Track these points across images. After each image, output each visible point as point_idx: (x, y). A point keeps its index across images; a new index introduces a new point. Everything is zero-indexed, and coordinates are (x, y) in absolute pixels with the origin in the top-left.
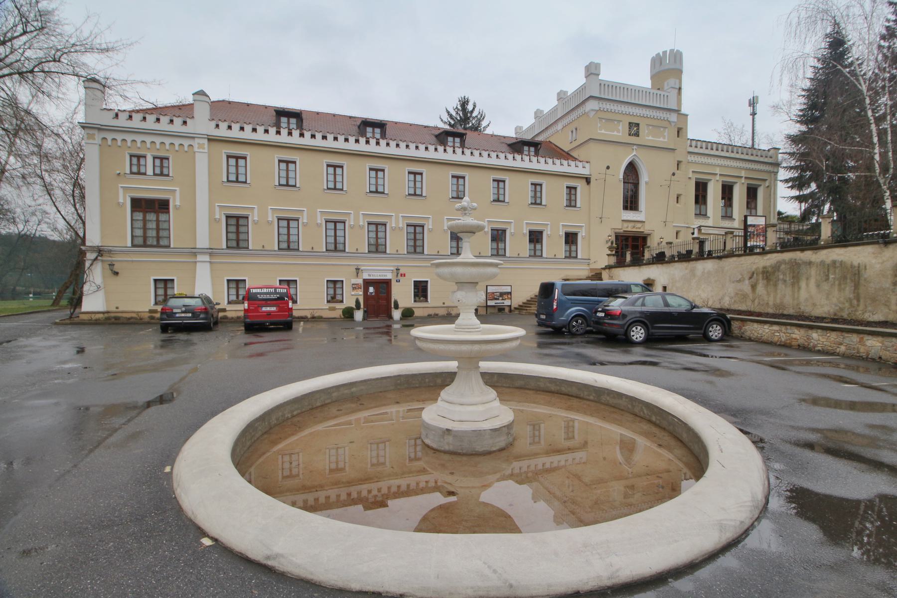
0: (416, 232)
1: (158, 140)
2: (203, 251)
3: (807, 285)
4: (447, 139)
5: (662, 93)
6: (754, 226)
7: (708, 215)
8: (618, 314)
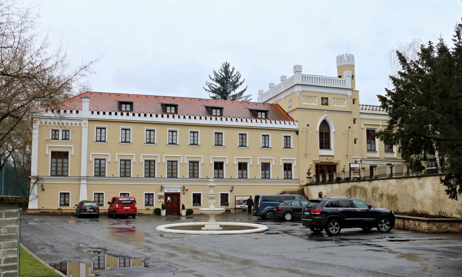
0: (194, 165)
2: (84, 178)
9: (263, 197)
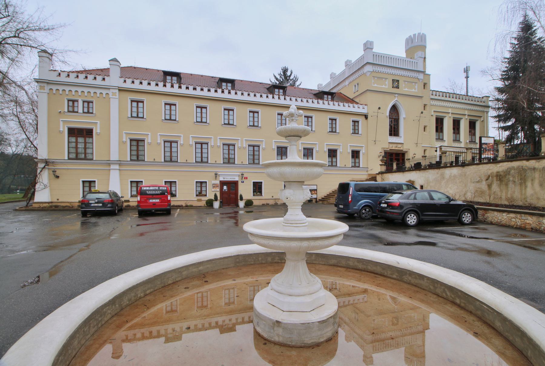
0: (254, 148)
1: (86, 90)
3: (532, 184)
4: (275, 90)
5: (414, 61)
6: (486, 144)
8: (397, 205)
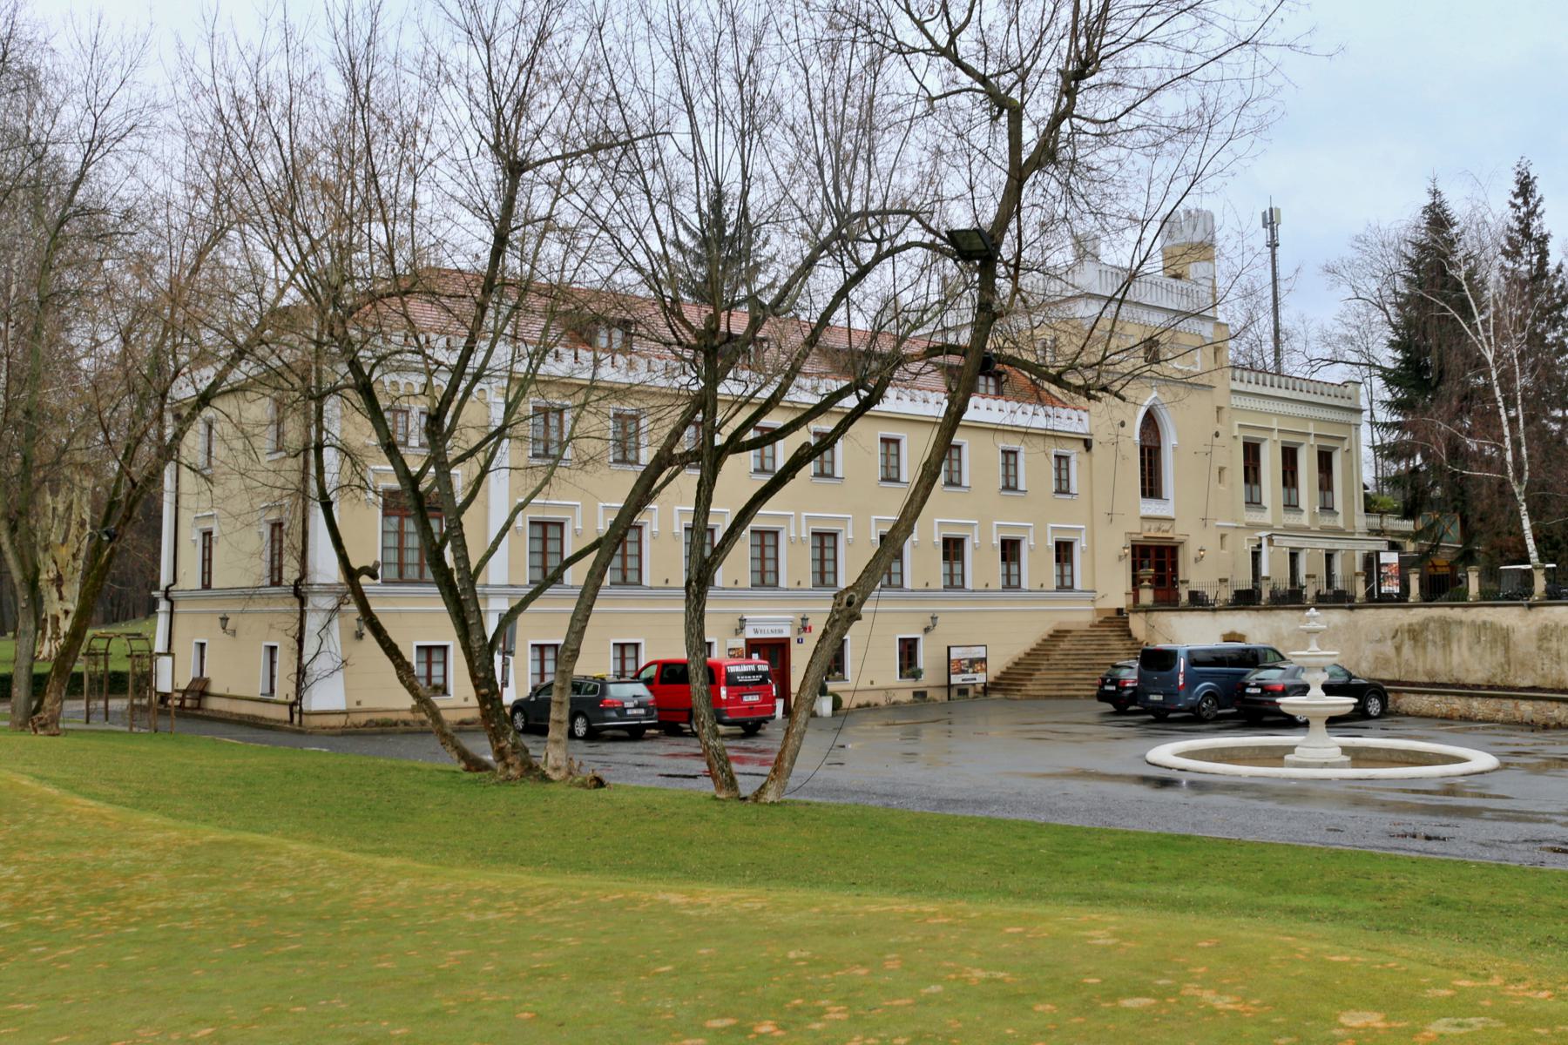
3: (1459, 647)
7: (1264, 503)
9: (1190, 653)
